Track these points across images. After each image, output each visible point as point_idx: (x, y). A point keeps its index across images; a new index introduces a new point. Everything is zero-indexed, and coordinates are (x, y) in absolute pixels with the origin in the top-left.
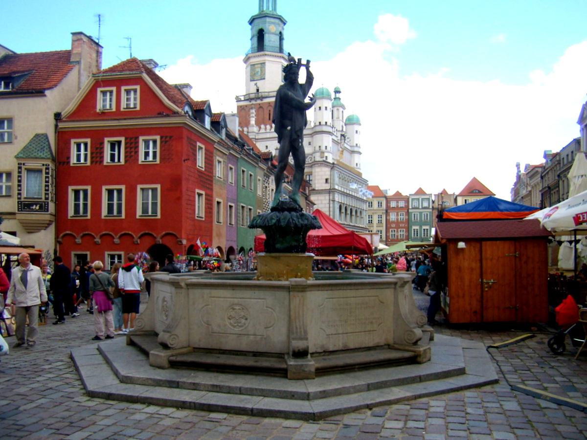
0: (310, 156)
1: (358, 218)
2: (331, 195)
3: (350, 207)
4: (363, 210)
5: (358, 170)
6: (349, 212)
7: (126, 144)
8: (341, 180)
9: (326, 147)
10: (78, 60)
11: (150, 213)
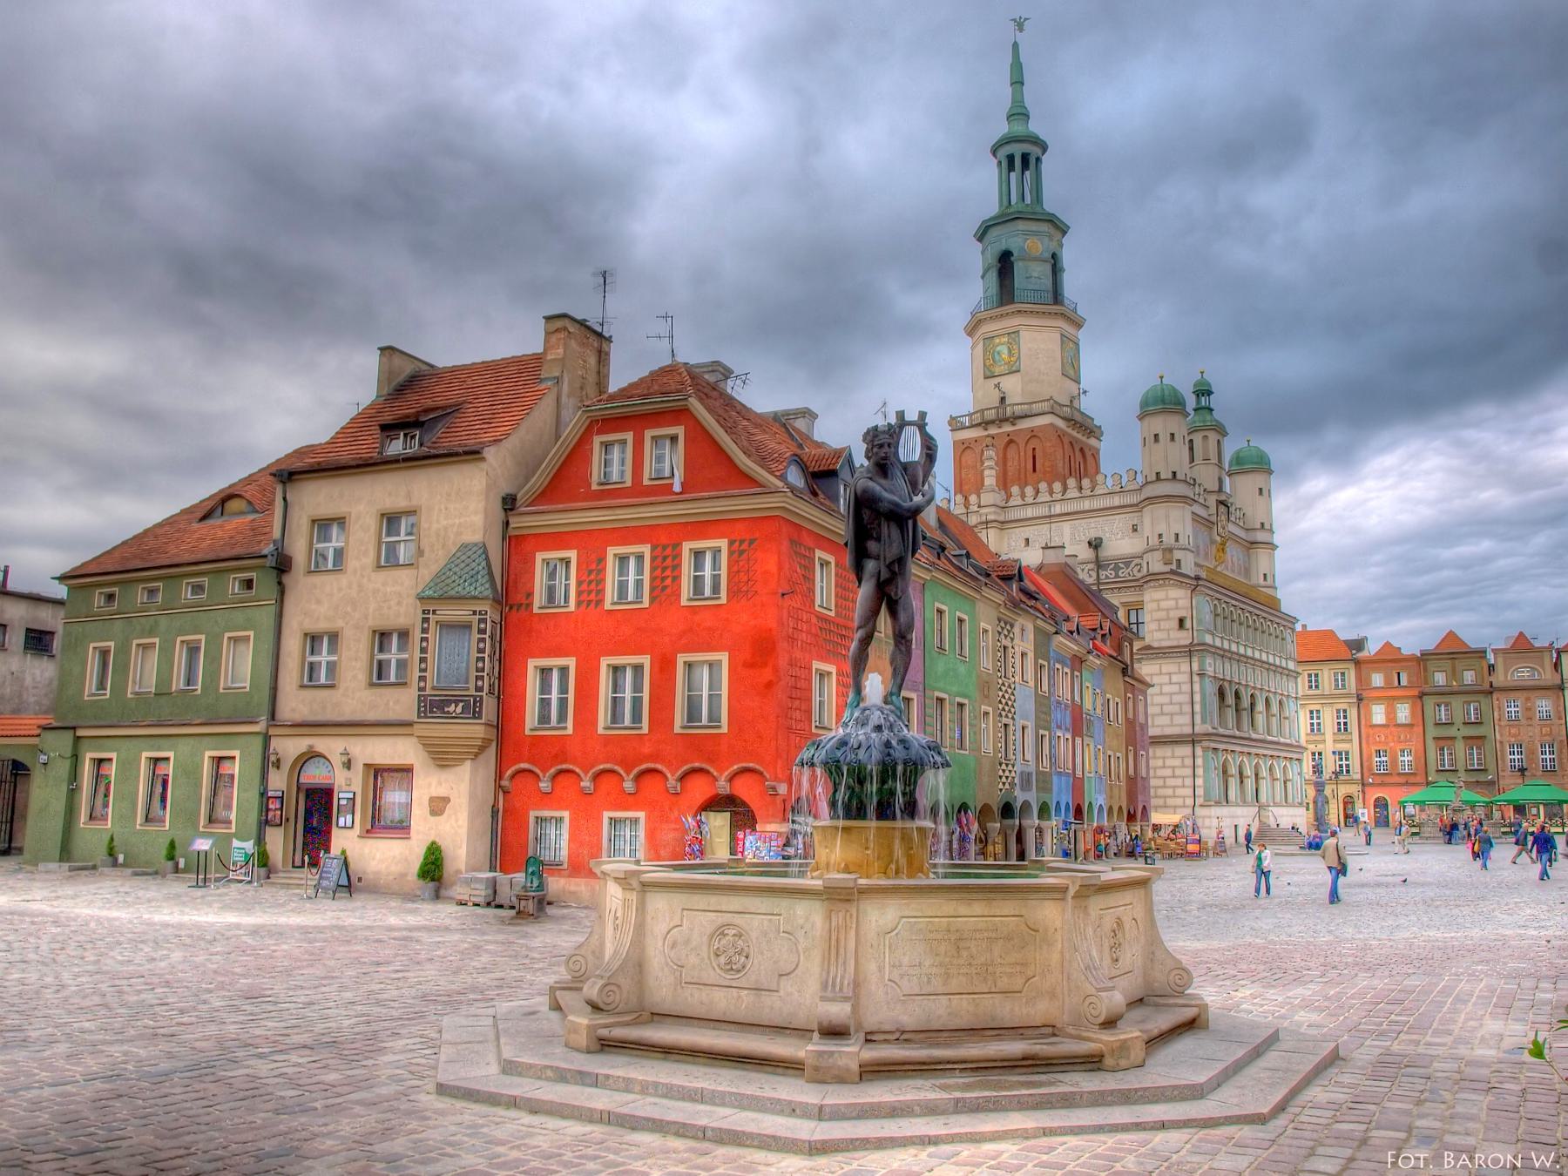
0: (1137, 561)
1: (1274, 719)
2: (1195, 659)
5: (1269, 591)
7: (653, 560)
8: (1219, 620)
9: (1177, 535)
10: (557, 374)
11: (705, 721)
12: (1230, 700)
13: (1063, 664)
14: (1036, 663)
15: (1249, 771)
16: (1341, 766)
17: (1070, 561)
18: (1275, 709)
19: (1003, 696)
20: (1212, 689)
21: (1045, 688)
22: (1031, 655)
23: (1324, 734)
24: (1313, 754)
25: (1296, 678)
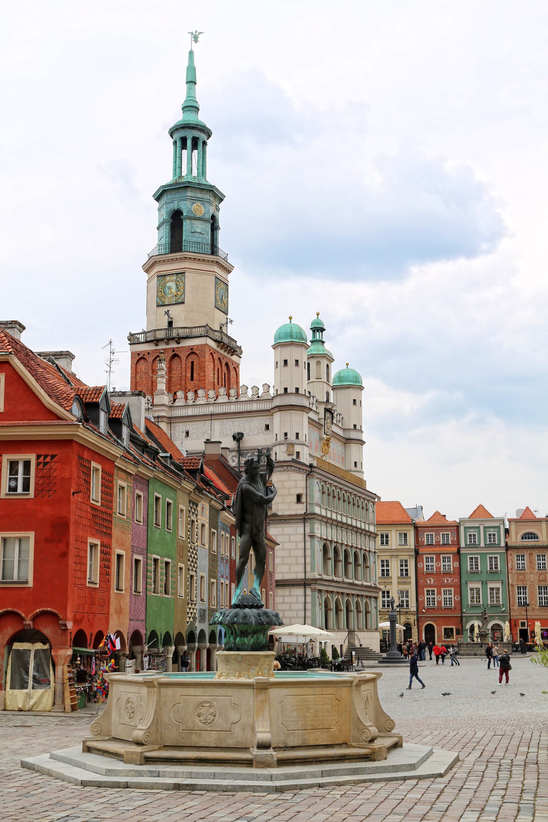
3: (344, 548)
4: (369, 551)
6: (342, 557)
8: (326, 495)
12: (331, 555)
13: (226, 531)
14: (210, 531)
15: (343, 607)
16: (402, 602)
17: (224, 452)
18: (361, 561)
19: (191, 556)
20: (318, 546)
21: (215, 548)
22: (207, 526)
23: (391, 578)
24: (384, 592)
25: (375, 538)
